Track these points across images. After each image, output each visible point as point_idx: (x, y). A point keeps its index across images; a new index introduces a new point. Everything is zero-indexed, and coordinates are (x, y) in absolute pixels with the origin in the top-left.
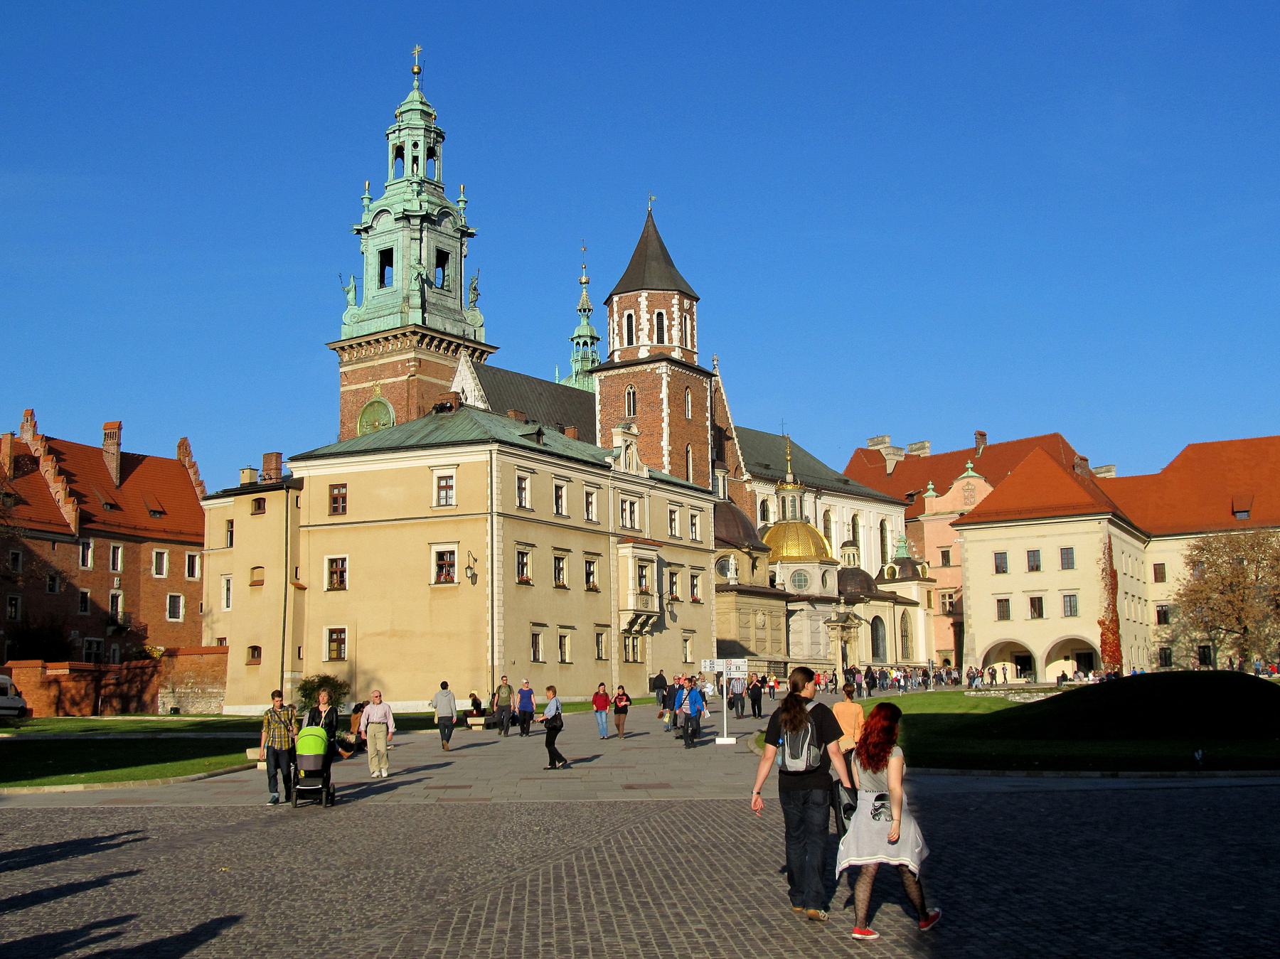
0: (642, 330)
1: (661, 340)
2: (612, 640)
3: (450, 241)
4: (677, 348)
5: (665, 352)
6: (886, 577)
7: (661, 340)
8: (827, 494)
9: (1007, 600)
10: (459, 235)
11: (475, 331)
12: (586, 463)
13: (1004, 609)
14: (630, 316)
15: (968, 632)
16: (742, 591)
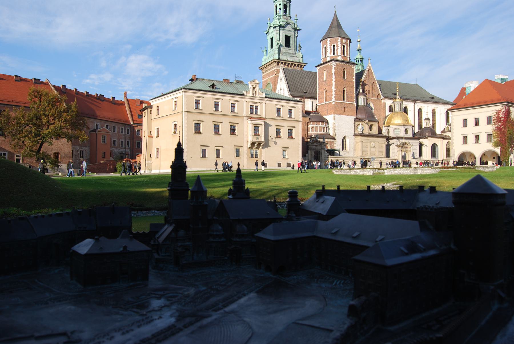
0: (328, 51)
1: (334, 54)
2: (245, 152)
3: (291, 32)
4: (339, 56)
5: (335, 58)
6: (446, 130)
7: (334, 54)
8: (419, 102)
9: (467, 137)
10: (294, 30)
11: (299, 59)
12: (230, 93)
13: (465, 140)
14: (325, 47)
15: (452, 149)
16: (362, 135)
